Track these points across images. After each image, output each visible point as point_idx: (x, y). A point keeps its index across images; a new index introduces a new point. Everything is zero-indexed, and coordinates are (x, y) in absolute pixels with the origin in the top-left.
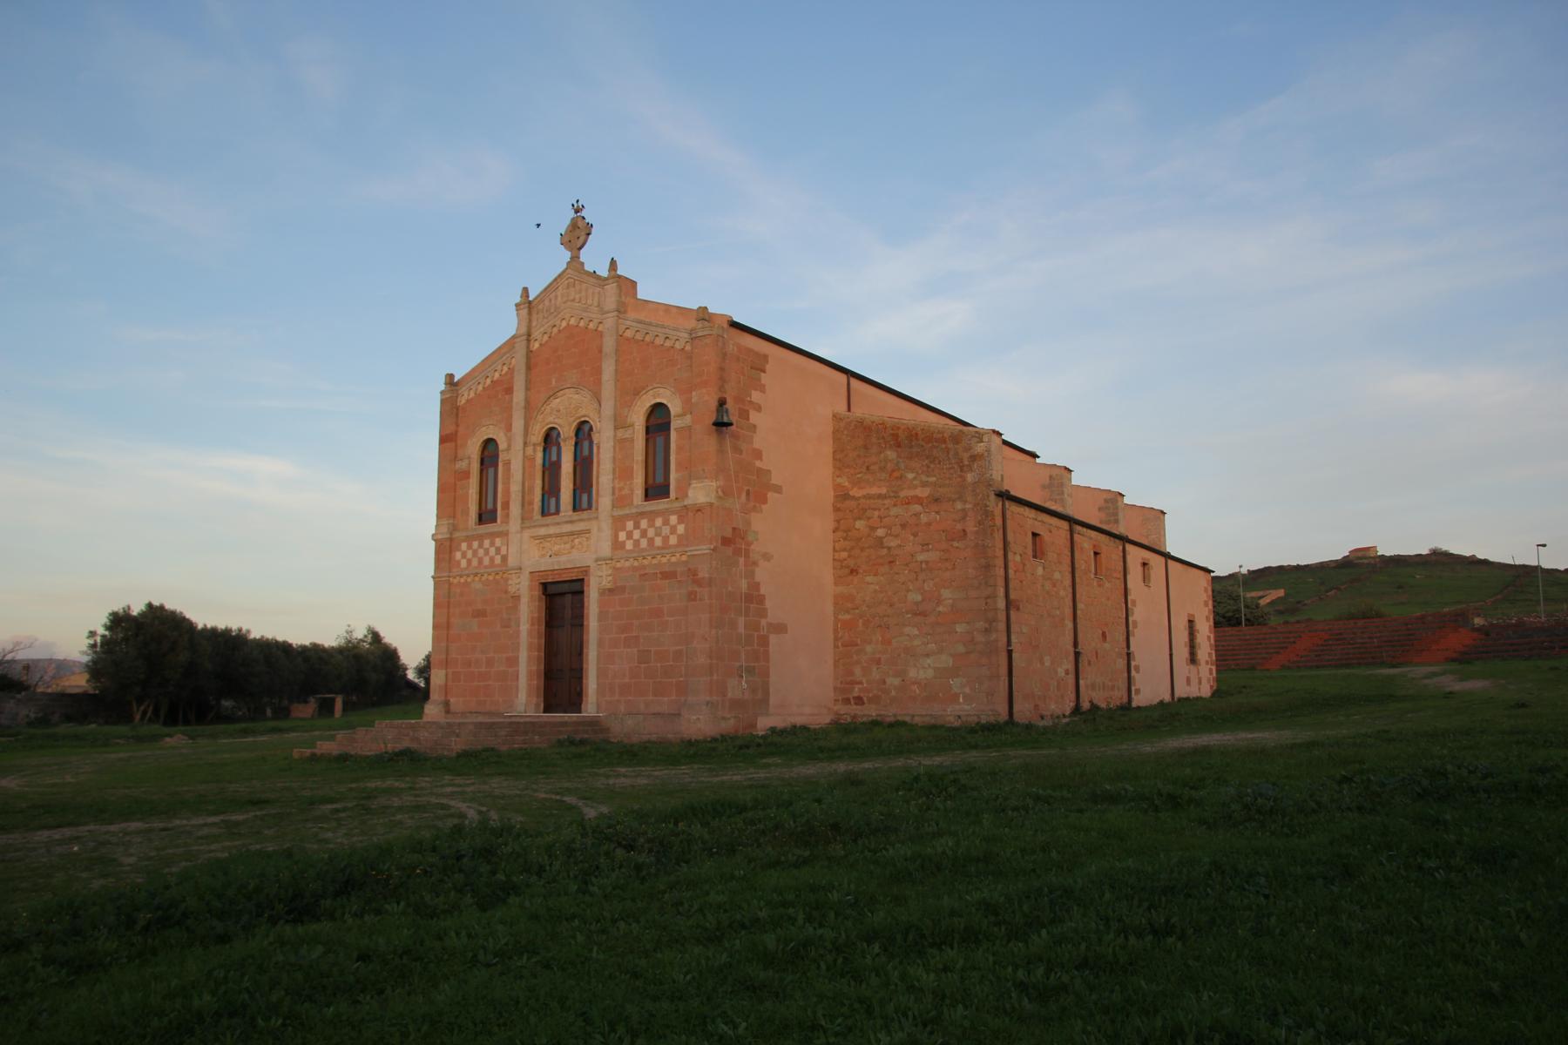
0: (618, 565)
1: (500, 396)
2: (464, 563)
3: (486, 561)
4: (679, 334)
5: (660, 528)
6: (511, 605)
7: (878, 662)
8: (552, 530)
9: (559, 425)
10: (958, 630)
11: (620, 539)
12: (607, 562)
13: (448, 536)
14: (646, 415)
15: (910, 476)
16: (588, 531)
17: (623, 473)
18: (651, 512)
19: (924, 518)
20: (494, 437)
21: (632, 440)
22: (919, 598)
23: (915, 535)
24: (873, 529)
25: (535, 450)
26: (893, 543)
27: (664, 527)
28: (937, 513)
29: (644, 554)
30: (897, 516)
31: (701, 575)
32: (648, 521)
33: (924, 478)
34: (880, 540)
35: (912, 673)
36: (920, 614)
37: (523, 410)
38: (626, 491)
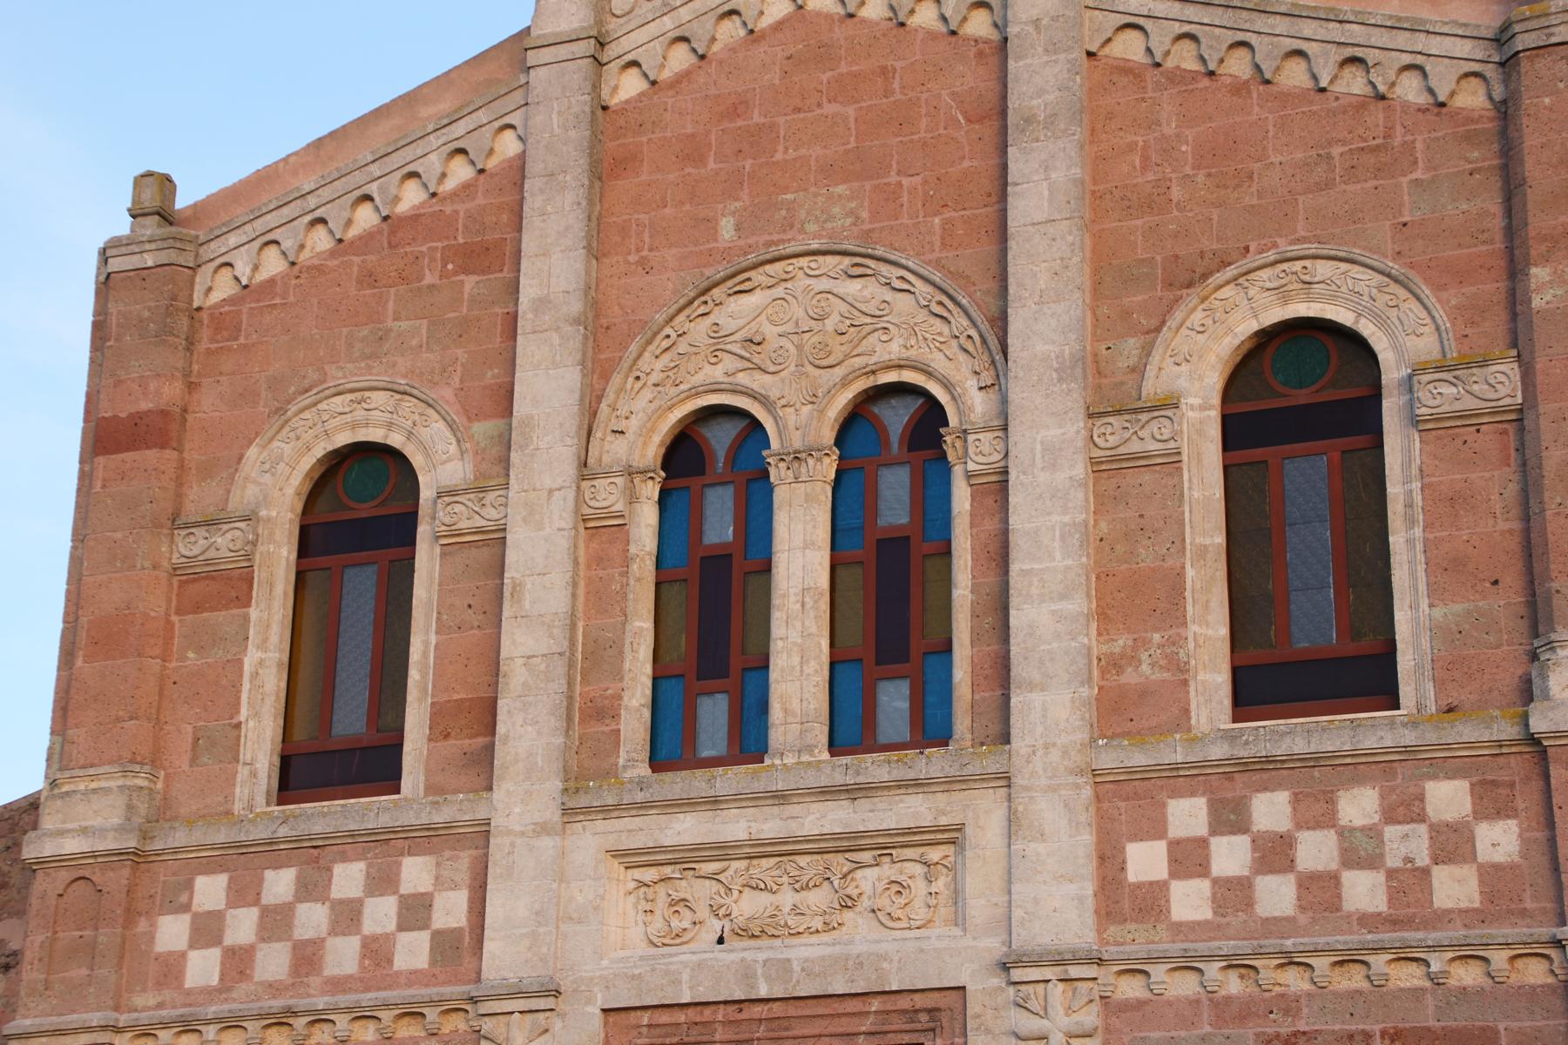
0: (1131, 989)
1: (429, 279)
2: (203, 968)
3: (343, 956)
4: (1421, 42)
5: (1372, 832)
8: (736, 826)
9: (753, 395)
11: (1134, 874)
12: (1074, 971)
13: (131, 843)
14: (1226, 375)
16: (953, 836)
18: (1313, 761)
20: (396, 440)
21: (1172, 462)
25: (632, 498)
27: (1391, 832)
29: (1289, 944)
32: (1296, 800)
37: (575, 335)
38: (1146, 671)
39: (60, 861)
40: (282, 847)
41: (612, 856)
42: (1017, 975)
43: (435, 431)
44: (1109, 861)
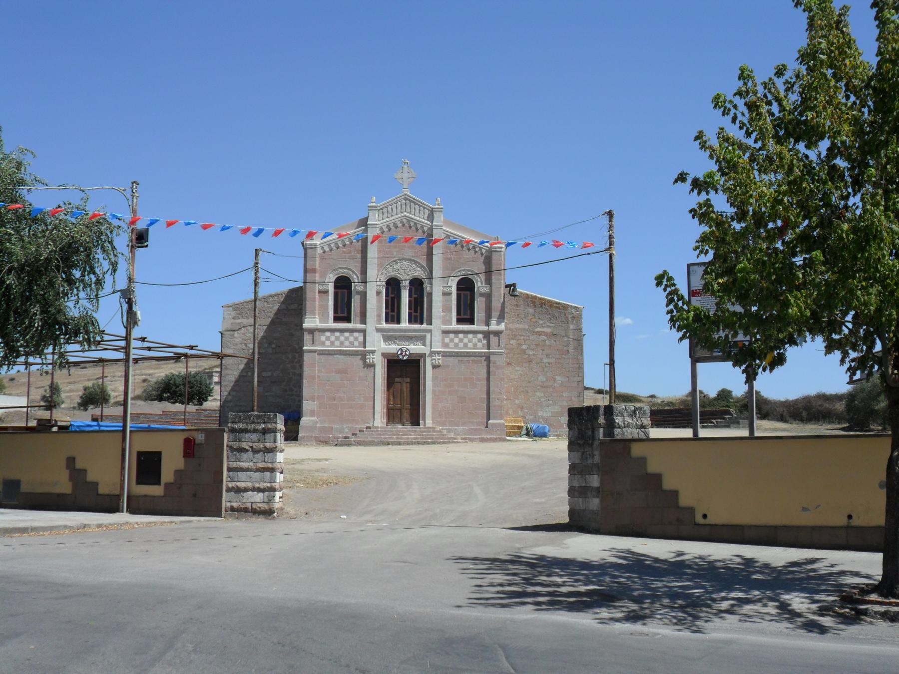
7: (522, 408)
10: (564, 395)
15: (541, 322)
17: (447, 309)
19: (548, 343)
22: (545, 380)
23: (543, 350)
24: (520, 345)
26: (531, 353)
28: (555, 341)
30: (533, 341)
31: (498, 363)
33: (548, 324)
34: (524, 351)
35: (540, 414)
36: (544, 387)
44: (443, 340)
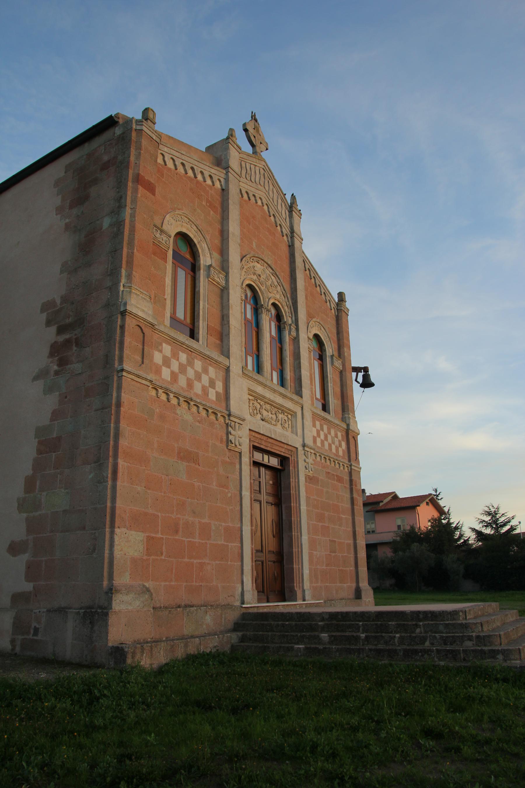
2: (166, 373)
3: (198, 388)
6: (228, 460)
39: (136, 316)
40: (184, 346)
41: (248, 390)
42: (306, 449)
43: (205, 246)
